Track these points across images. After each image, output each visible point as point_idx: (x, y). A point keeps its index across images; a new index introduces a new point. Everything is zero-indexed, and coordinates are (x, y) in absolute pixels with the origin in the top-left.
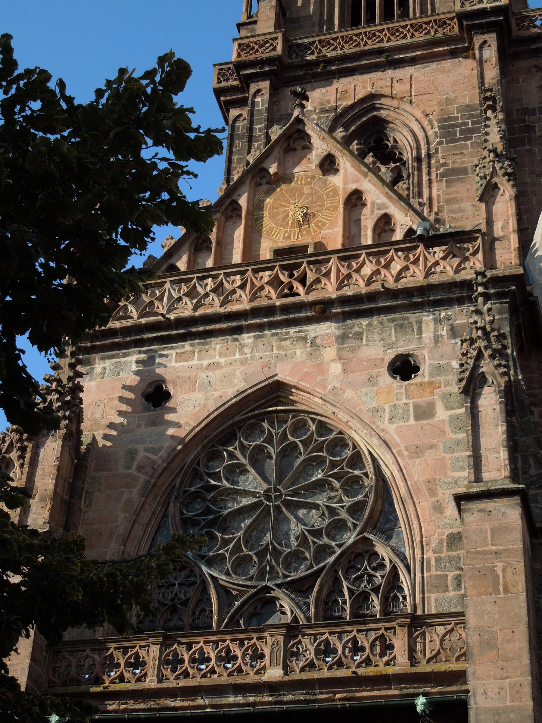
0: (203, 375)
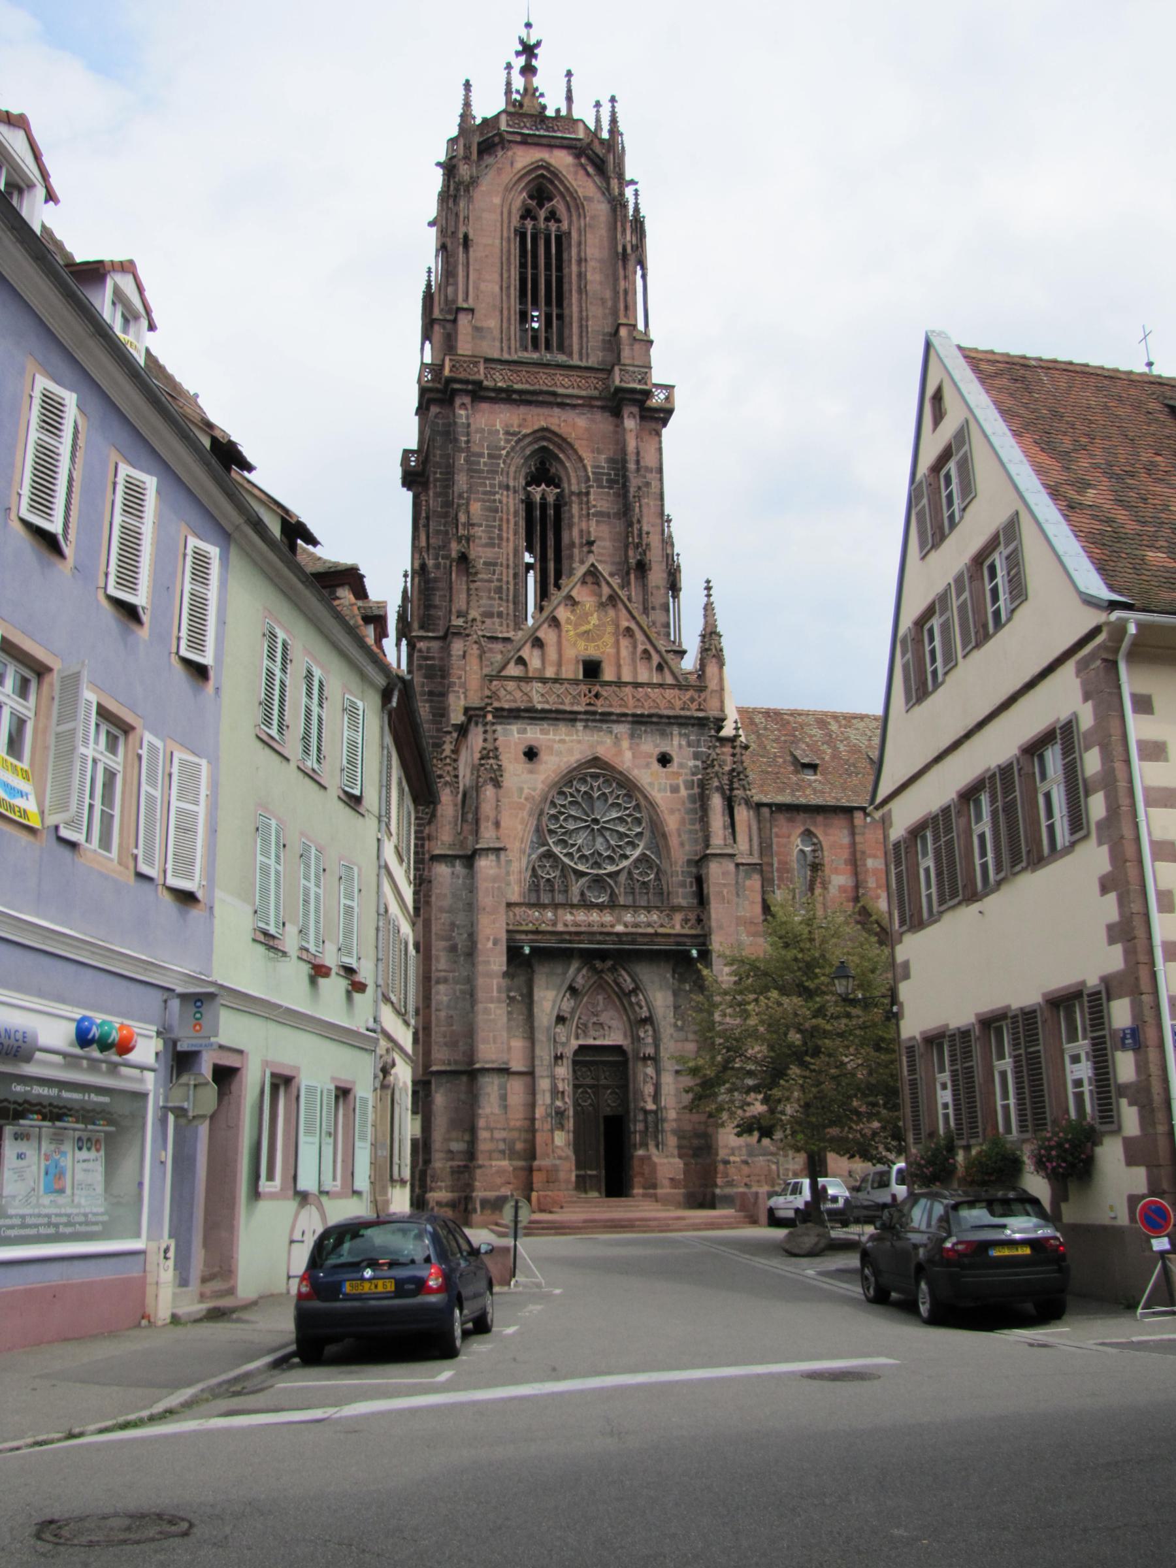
0: (556, 746)
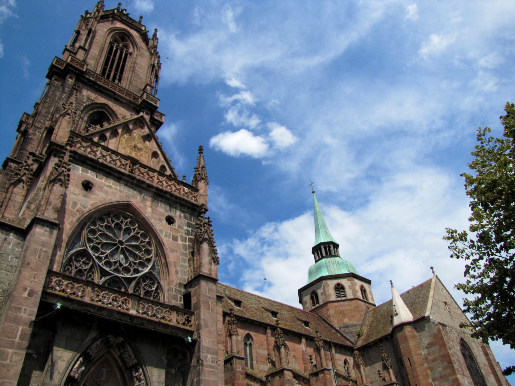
0: (105, 188)
